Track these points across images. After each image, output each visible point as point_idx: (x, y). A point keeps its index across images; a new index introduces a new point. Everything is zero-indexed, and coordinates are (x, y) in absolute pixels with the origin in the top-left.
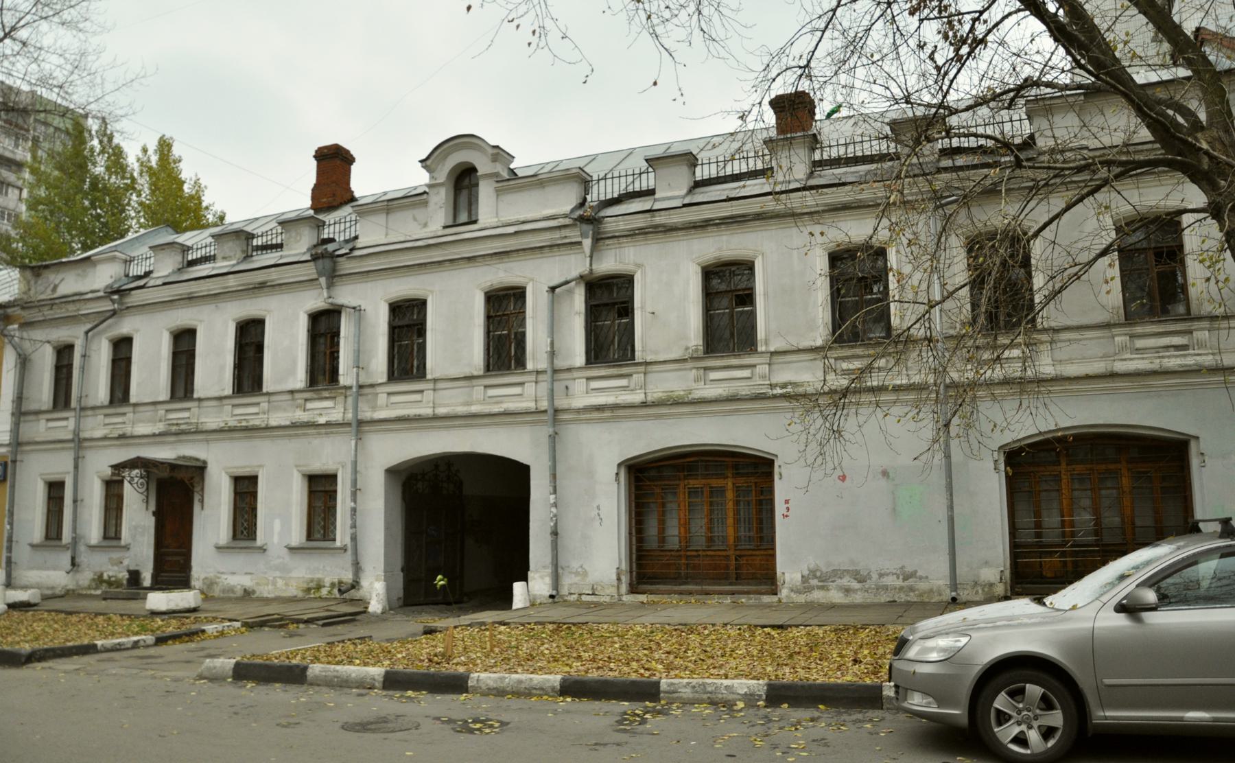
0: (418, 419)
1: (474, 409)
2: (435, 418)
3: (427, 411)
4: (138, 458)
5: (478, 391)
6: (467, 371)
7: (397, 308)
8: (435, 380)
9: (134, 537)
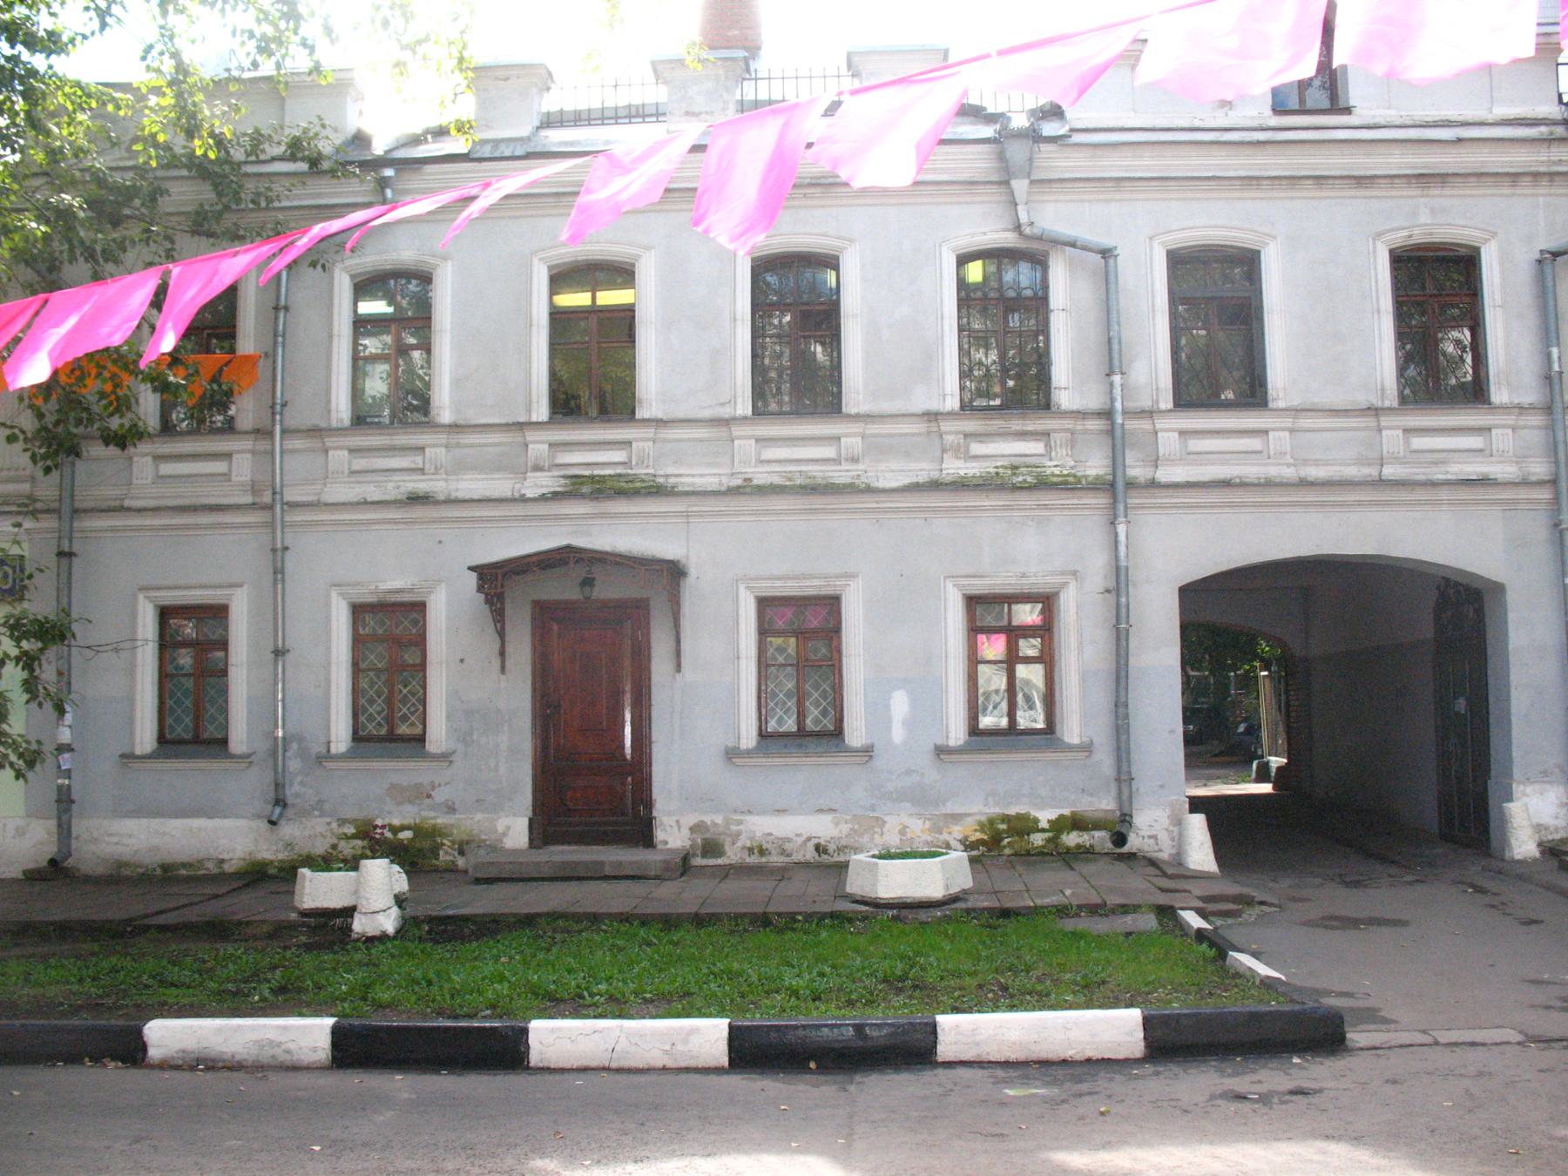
0: (1268, 484)
1: (1389, 471)
2: (1304, 484)
3: (1289, 473)
4: (568, 548)
5: (1392, 439)
6: (1362, 399)
7: (1186, 264)
8: (1297, 411)
9: (465, 738)
